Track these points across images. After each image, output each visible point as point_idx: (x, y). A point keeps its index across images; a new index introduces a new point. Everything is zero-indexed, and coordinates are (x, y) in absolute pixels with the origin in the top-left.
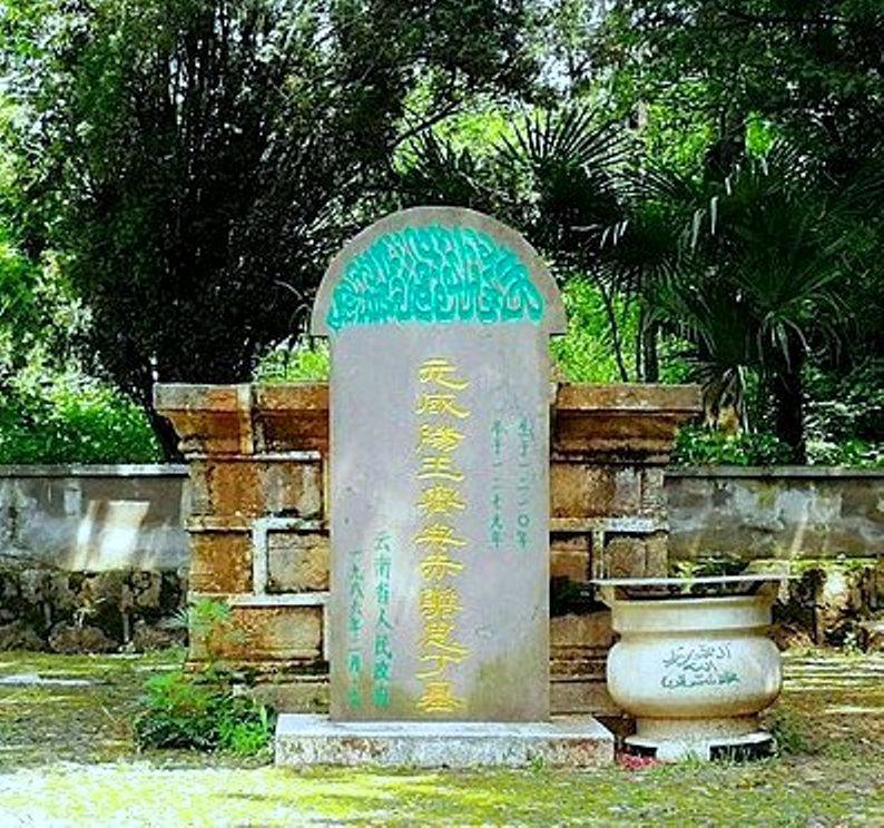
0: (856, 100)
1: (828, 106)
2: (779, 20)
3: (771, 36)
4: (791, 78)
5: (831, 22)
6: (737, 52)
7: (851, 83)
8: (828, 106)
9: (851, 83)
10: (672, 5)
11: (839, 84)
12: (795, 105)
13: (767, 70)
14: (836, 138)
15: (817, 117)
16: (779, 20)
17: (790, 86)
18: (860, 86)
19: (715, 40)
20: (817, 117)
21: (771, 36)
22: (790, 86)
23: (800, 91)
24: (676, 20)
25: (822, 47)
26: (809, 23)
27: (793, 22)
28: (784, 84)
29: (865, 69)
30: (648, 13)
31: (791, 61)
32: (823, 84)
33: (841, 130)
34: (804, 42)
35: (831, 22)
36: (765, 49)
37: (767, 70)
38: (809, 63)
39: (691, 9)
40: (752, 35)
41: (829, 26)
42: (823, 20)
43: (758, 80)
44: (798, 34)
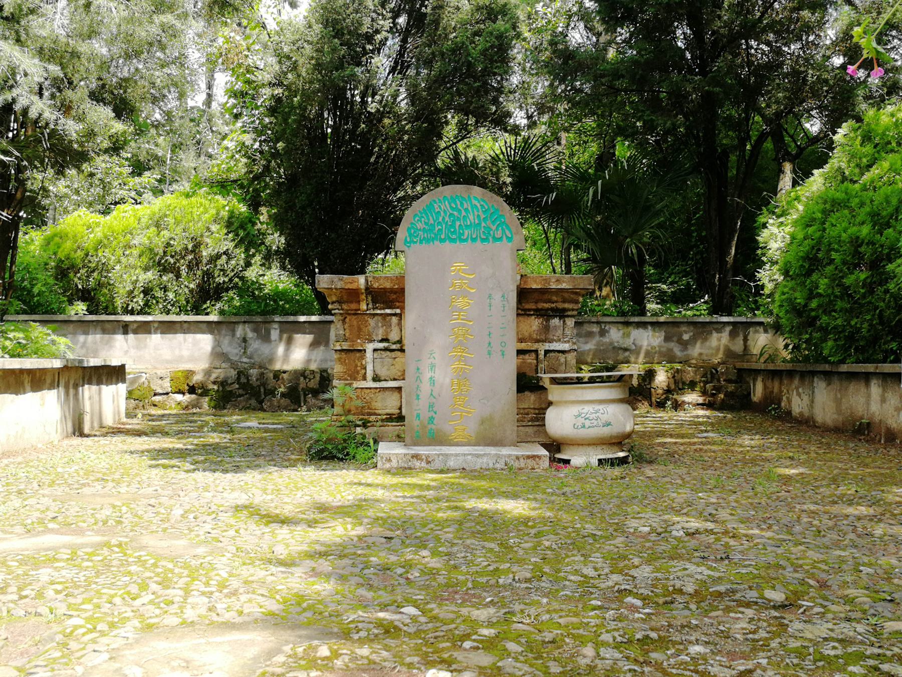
0: (672, 130)
1: (658, 134)
2: (633, 91)
3: (628, 99)
4: (638, 120)
5: (659, 92)
6: (612, 106)
7: (669, 122)
8: (658, 134)
9: (669, 122)
10: (578, 83)
11: (662, 123)
12: (641, 133)
13: (626, 116)
14: (661, 149)
15: (652, 140)
16: (633, 91)
17: (638, 124)
18: (674, 124)
19: (600, 101)
20: (652, 140)
21: (628, 99)
22: (638, 124)
23: (644, 126)
24: (580, 91)
25: (654, 104)
26: (648, 92)
27: (640, 92)
28: (635, 123)
29: (677, 115)
30: (567, 87)
31: (639, 111)
32: (655, 123)
33: (664, 146)
34: (645, 102)
35: (659, 92)
36: (625, 106)
37: (626, 116)
38: (648, 112)
39: (588, 85)
40: (619, 98)
41: (658, 95)
42: (655, 91)
43: (622, 121)
44: (642, 98)
